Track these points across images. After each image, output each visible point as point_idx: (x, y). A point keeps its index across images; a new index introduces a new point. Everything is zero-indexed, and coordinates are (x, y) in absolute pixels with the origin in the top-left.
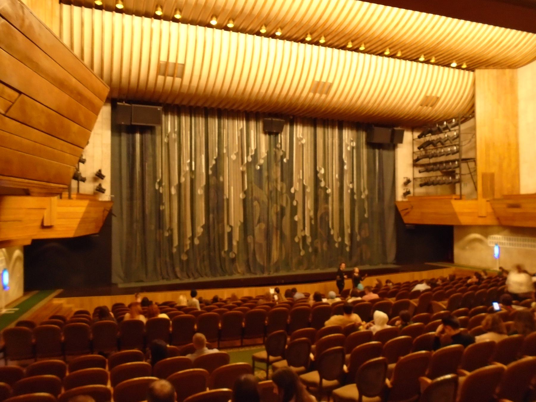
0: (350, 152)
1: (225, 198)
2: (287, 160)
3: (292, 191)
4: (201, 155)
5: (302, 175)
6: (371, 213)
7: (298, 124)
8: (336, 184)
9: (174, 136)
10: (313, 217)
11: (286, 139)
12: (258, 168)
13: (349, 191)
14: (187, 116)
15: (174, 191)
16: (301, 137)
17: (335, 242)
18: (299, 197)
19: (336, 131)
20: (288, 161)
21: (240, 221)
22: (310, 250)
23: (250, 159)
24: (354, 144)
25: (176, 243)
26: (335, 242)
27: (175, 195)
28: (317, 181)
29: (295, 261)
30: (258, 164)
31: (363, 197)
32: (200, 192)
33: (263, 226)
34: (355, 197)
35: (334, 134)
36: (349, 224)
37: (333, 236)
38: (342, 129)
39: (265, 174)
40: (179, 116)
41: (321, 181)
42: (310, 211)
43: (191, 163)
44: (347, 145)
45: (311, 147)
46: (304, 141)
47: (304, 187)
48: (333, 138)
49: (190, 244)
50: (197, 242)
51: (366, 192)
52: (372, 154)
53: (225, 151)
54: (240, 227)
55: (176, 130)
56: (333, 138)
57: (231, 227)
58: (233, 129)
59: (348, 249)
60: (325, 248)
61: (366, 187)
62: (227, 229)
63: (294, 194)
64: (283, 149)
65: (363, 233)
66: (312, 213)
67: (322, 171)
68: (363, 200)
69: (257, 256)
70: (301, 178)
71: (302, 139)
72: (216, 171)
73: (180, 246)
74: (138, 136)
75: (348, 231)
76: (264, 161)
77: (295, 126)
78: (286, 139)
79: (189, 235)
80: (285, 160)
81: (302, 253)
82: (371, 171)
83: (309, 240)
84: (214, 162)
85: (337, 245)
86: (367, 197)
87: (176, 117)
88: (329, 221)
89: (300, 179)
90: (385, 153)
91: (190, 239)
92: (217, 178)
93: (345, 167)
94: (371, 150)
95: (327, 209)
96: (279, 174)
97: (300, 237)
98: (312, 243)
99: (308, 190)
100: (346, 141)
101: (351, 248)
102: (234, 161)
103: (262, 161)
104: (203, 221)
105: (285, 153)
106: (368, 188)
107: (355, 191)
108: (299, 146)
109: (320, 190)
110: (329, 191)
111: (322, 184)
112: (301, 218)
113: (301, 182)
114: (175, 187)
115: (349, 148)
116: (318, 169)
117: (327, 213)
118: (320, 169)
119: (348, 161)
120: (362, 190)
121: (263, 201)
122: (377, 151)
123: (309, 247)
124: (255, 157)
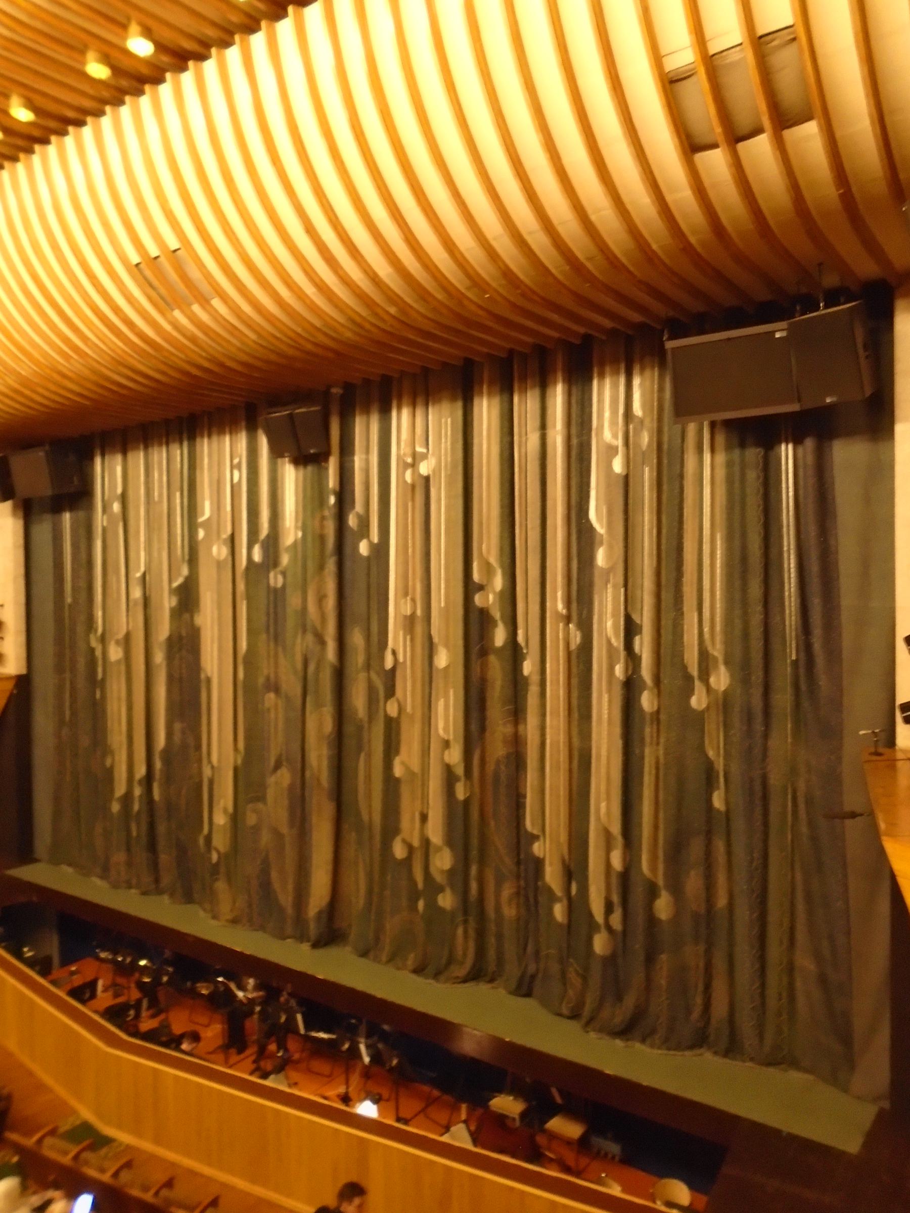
0: (626, 478)
1: (203, 676)
2: (371, 544)
3: (389, 663)
4: (160, 551)
5: (420, 599)
6: (759, 795)
7: (405, 400)
8: (561, 636)
9: (116, 507)
10: (460, 771)
11: (367, 471)
12: (280, 581)
13: (619, 671)
14: (138, 448)
15: (115, 653)
16: (420, 449)
17: (552, 898)
18: (408, 689)
19: (558, 395)
20: (373, 547)
21: (236, 749)
22: (446, 900)
23: (257, 556)
24: (645, 439)
25: (120, 790)
26: (552, 898)
27: (118, 662)
28: (476, 623)
29: (392, 925)
30: (279, 569)
31: (698, 701)
32: (159, 657)
33: (284, 777)
34: (647, 701)
35: (549, 412)
36: (616, 829)
37: (539, 864)
38: (590, 380)
39: (294, 601)
40: (124, 453)
41: (495, 624)
42: (447, 744)
43: (144, 575)
44: (611, 451)
45: (450, 484)
46: (424, 469)
47: (430, 649)
48: (543, 427)
49: (141, 796)
50: (156, 795)
51: (721, 679)
52: (753, 476)
53: (201, 534)
54: (236, 770)
55: (119, 490)
56: (543, 427)
57: (213, 767)
58: (220, 464)
59: (600, 944)
60: (509, 912)
61: (717, 651)
62: (207, 772)
63: (394, 670)
64: (359, 507)
65: (693, 883)
66: (455, 756)
67: (499, 582)
68: (699, 718)
69: (274, 875)
70: (419, 612)
71: (424, 457)
72: (187, 597)
73: (127, 798)
74: (67, 517)
75: (603, 861)
76: (294, 559)
77: (394, 414)
78: (367, 471)
79: (141, 771)
80: (364, 548)
81: (421, 904)
82: (754, 565)
83: (443, 861)
84: (185, 571)
85: (559, 912)
86: (725, 703)
87: (119, 458)
88: (525, 797)
89: (410, 620)
90: (847, 454)
91: (140, 782)
92: (192, 617)
93: (601, 558)
94: (753, 454)
95: (517, 743)
96: (331, 602)
97: (416, 843)
98: (459, 876)
99: (442, 659)
100: (607, 435)
101: (622, 939)
102: (219, 564)
103: (285, 559)
104: (161, 740)
105: (364, 522)
106: (726, 663)
107: (646, 672)
108: (413, 487)
109: (493, 659)
110: (528, 667)
111: (500, 637)
112: (416, 767)
113: (419, 629)
114: (118, 642)
115: (618, 466)
116: (476, 577)
117: (517, 760)
118: (488, 569)
119: (610, 526)
120: (694, 671)
121: (287, 697)
122: (787, 453)
123: (441, 889)
124: (272, 544)
